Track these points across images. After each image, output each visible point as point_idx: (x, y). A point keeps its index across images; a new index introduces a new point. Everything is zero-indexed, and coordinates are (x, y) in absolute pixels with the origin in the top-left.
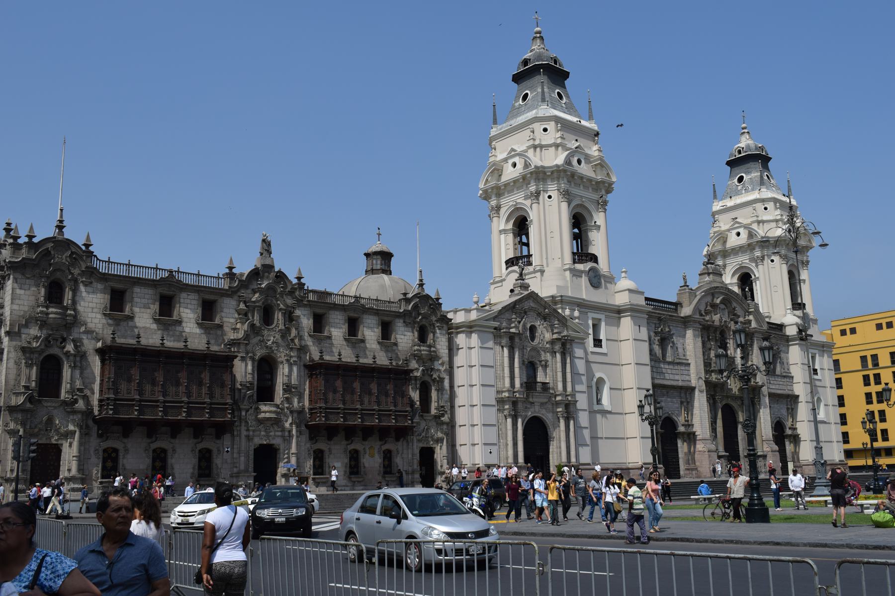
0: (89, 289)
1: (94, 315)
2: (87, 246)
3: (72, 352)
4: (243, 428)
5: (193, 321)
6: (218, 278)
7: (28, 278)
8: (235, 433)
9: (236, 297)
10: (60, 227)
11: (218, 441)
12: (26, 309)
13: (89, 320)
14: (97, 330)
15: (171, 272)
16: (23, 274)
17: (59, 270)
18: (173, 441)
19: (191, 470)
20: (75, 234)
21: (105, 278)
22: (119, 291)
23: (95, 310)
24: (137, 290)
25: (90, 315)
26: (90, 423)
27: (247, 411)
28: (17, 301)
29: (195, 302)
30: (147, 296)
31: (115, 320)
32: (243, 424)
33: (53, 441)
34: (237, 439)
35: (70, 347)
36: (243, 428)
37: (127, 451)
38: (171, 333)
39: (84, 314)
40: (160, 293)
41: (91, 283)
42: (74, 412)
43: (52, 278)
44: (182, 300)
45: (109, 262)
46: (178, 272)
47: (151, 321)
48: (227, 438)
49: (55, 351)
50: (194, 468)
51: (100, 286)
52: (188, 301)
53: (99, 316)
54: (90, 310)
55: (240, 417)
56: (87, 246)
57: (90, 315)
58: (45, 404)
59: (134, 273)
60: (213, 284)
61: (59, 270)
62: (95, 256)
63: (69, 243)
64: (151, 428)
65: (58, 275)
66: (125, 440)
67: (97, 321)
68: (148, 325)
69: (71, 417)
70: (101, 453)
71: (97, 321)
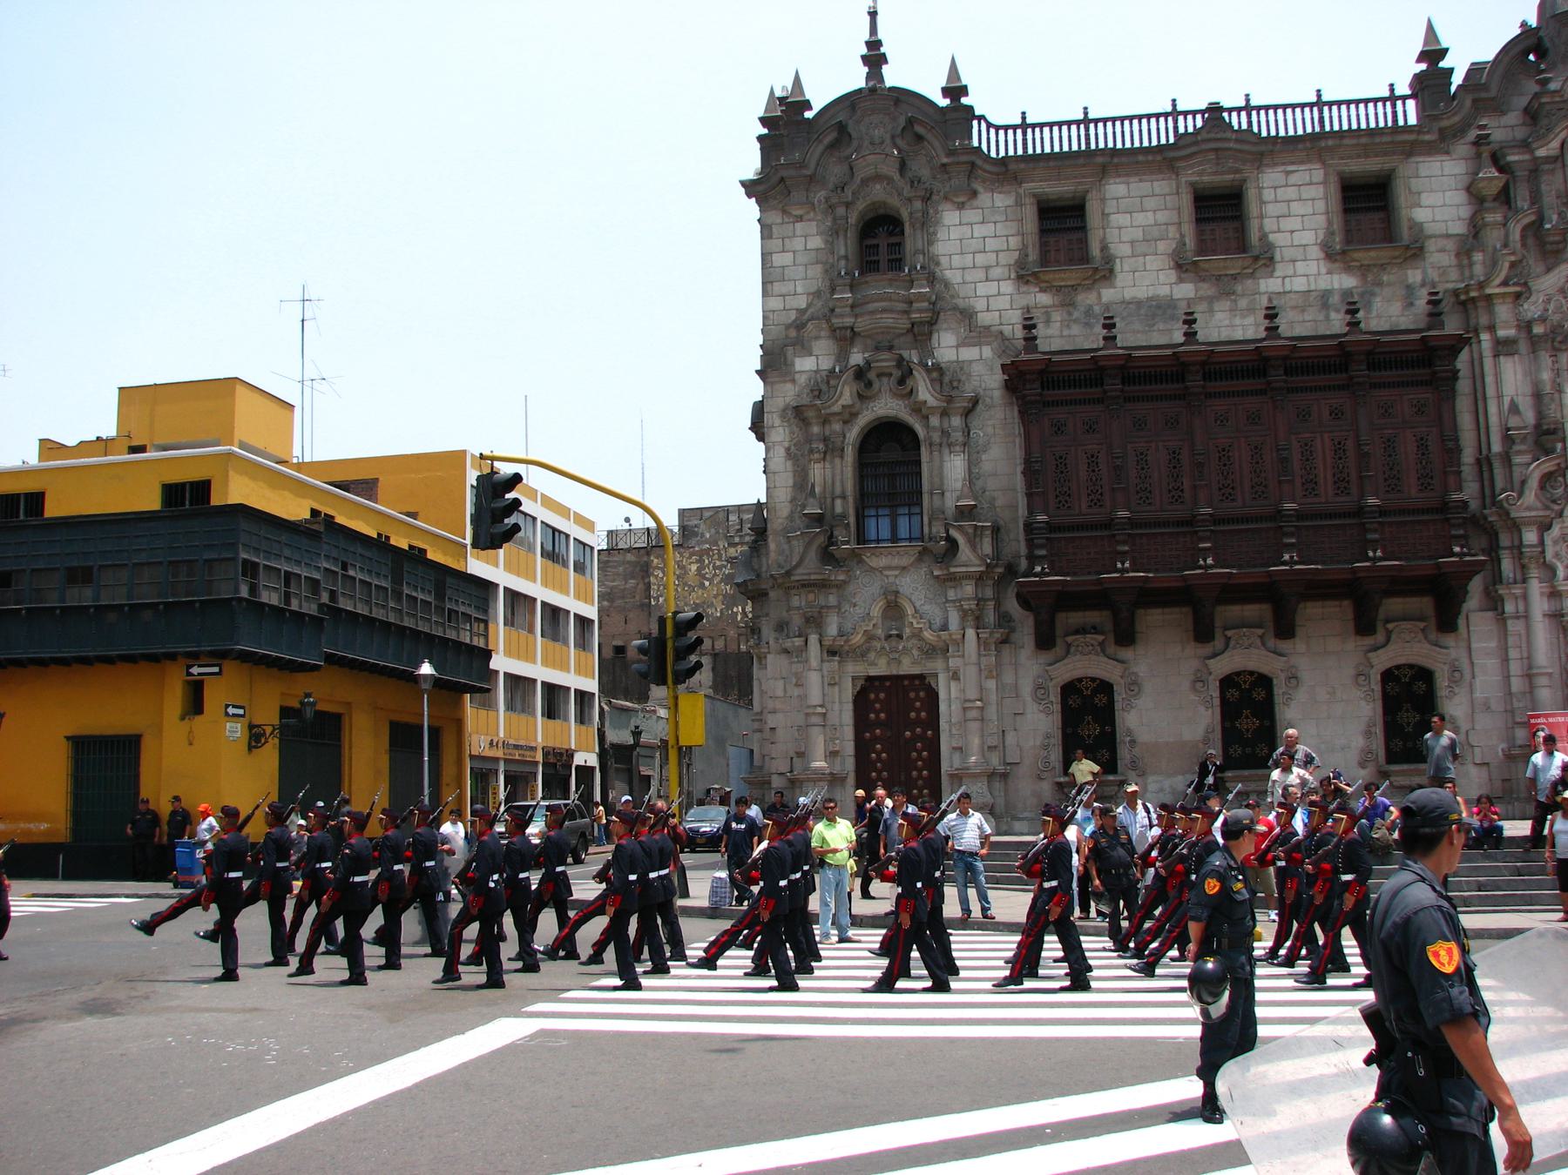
0: (971, 215)
1: (992, 288)
2: (955, 91)
3: (932, 402)
4: (1536, 587)
5: (1315, 252)
6: (1393, 98)
7: (800, 219)
8: (1509, 608)
9: (1463, 148)
10: (874, 58)
11: (1449, 640)
12: (802, 302)
13: (980, 305)
14: (1007, 330)
15: (1215, 110)
16: (784, 212)
17: (878, 178)
18: (1284, 645)
19: (1359, 742)
20: (915, 72)
21: (1008, 171)
22: (1061, 199)
23: (997, 272)
24: (1116, 188)
25: (982, 289)
26: (1012, 606)
27: (1544, 527)
28: (778, 287)
29: (1318, 191)
30: (1150, 203)
31: (1059, 289)
32: (1534, 573)
33: (907, 667)
34: (1514, 626)
35: (925, 393)
36: (1536, 587)
37: (1134, 686)
38: (1243, 303)
39: (964, 291)
40: (1192, 184)
41: (974, 194)
42: (953, 580)
43: (861, 205)
44: (1268, 195)
45: (1024, 126)
46: (1248, 108)
47: (1172, 275)
48: (1477, 624)
49: (887, 406)
50: (1368, 734)
51: (1002, 200)
52: (1291, 193)
53: (1008, 287)
54: (981, 275)
55: (1518, 549)
56: (955, 91)
57: (982, 289)
58: (875, 562)
59: (1103, 138)
60: (1377, 117)
61: (878, 178)
62: (981, 118)
63: (904, 97)
64: (1202, 616)
65: (878, 192)
66: (1126, 653)
67: (1003, 302)
68: (1164, 291)
69: (951, 594)
70: (1055, 697)
71: (1003, 302)
